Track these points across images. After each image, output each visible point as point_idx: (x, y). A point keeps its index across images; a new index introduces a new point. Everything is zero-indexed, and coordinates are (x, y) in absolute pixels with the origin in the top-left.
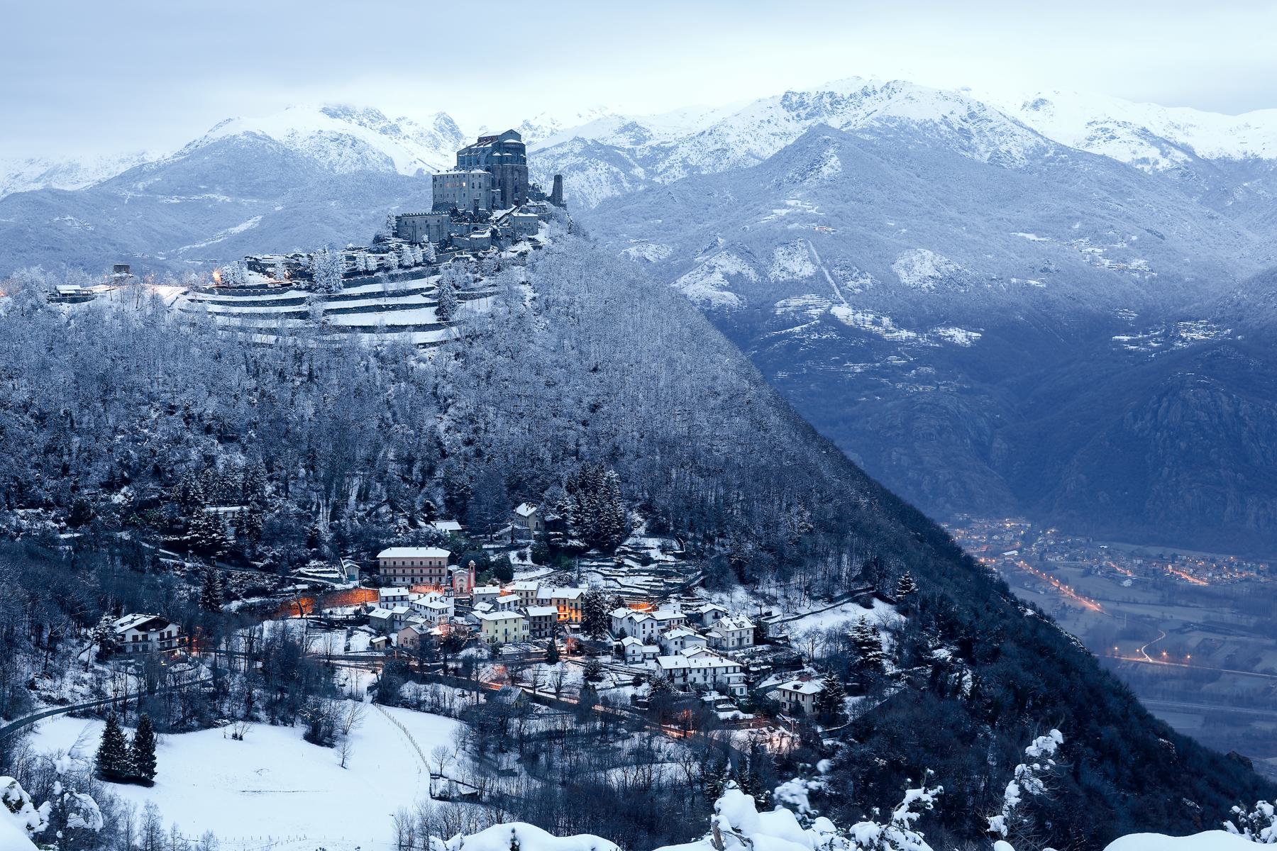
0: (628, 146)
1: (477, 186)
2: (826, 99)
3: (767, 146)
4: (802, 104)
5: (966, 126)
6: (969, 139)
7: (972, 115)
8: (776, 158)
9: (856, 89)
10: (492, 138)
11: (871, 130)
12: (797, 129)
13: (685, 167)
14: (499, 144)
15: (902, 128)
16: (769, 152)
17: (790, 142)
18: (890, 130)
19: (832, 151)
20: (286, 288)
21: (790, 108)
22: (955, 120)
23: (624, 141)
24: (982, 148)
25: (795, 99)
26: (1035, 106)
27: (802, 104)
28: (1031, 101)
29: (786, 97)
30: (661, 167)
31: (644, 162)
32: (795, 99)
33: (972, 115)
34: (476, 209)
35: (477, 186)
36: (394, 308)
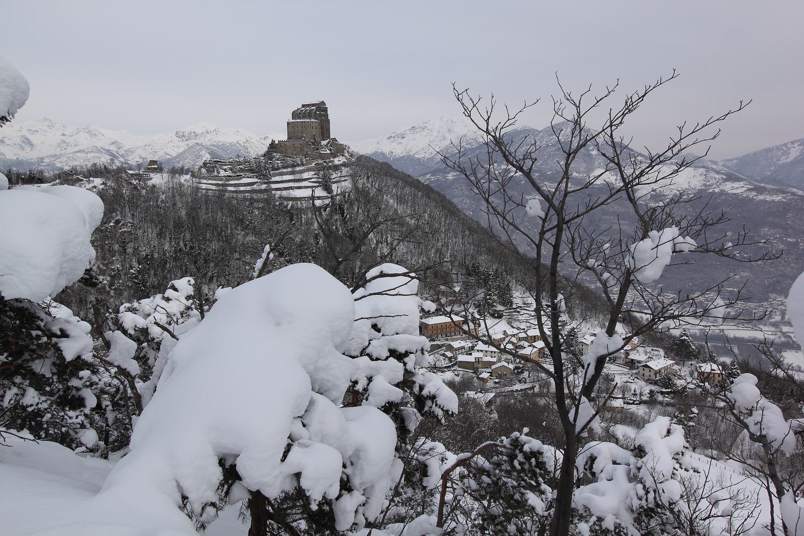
0: (115, 150)
1: (314, 127)
2: (193, 134)
3: (171, 151)
4: (183, 136)
5: (245, 145)
6: (247, 149)
7: (247, 141)
8: (181, 154)
9: (204, 130)
10: (313, 105)
11: (213, 145)
12: (182, 146)
13: (140, 158)
14: (318, 107)
15: (223, 145)
16: (174, 155)
17: (181, 150)
18: (220, 146)
19: (203, 152)
20: (239, 177)
21: (179, 137)
22: (241, 142)
23: (113, 148)
24: (252, 152)
25: (180, 134)
26: (265, 139)
27: (183, 136)
28: (263, 137)
29: (177, 133)
30: (130, 158)
31: (122, 156)
32: (180, 134)
33: (247, 141)
34: (314, 139)
35: (314, 127)
36: (300, 188)
